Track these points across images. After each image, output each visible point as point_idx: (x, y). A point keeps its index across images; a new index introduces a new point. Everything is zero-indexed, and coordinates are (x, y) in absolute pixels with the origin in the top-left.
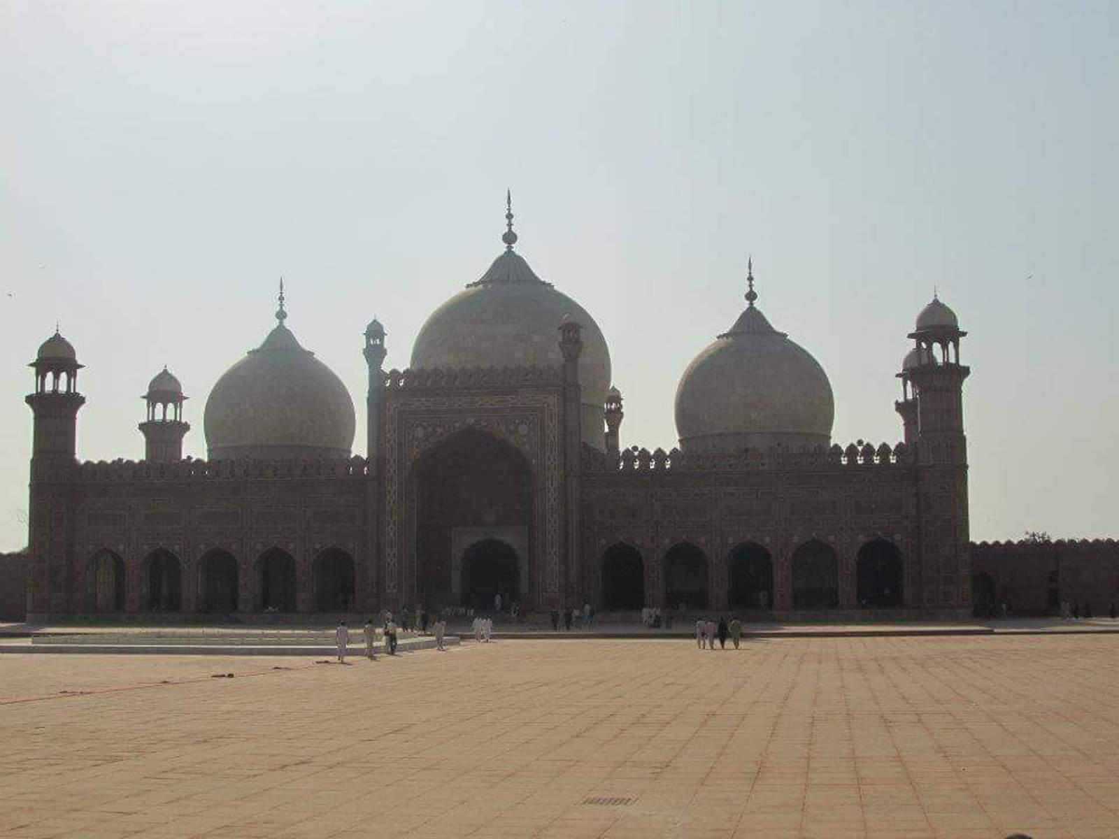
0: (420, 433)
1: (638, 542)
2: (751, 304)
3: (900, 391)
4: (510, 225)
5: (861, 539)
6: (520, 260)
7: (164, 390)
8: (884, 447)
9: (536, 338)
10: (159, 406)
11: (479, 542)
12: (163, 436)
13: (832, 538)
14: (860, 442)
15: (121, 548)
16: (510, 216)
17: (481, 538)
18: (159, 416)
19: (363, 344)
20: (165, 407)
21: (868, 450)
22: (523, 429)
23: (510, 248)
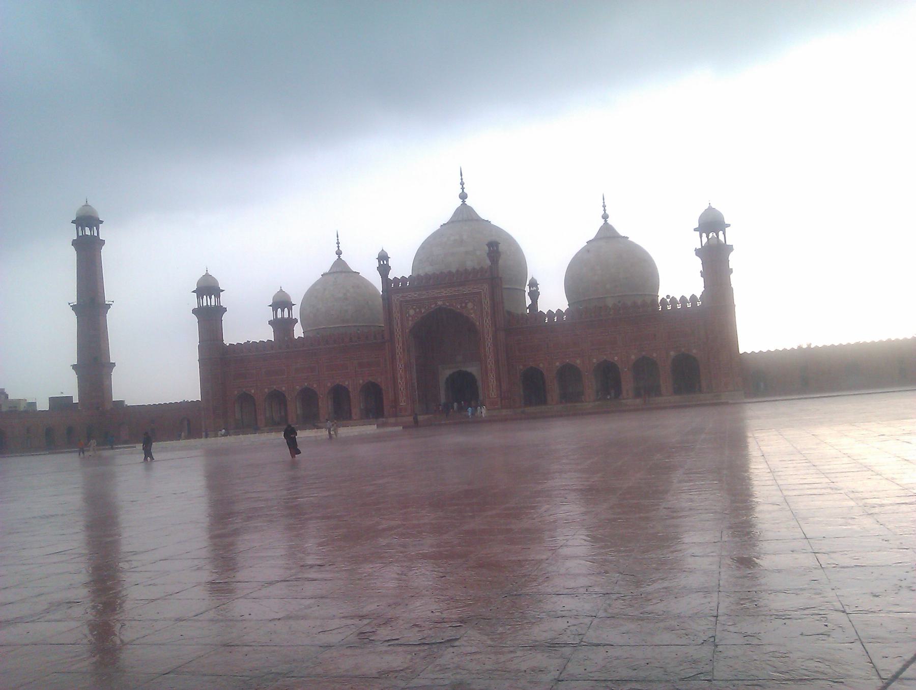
0: (412, 312)
1: (541, 365)
3: (697, 264)
4: (463, 189)
5: (672, 353)
6: (470, 210)
7: (281, 302)
8: (693, 297)
9: (478, 253)
11: (454, 373)
12: (282, 326)
13: (655, 355)
14: (668, 296)
16: (462, 184)
17: (455, 370)
18: (279, 316)
20: (283, 311)
21: (673, 300)
23: (464, 202)
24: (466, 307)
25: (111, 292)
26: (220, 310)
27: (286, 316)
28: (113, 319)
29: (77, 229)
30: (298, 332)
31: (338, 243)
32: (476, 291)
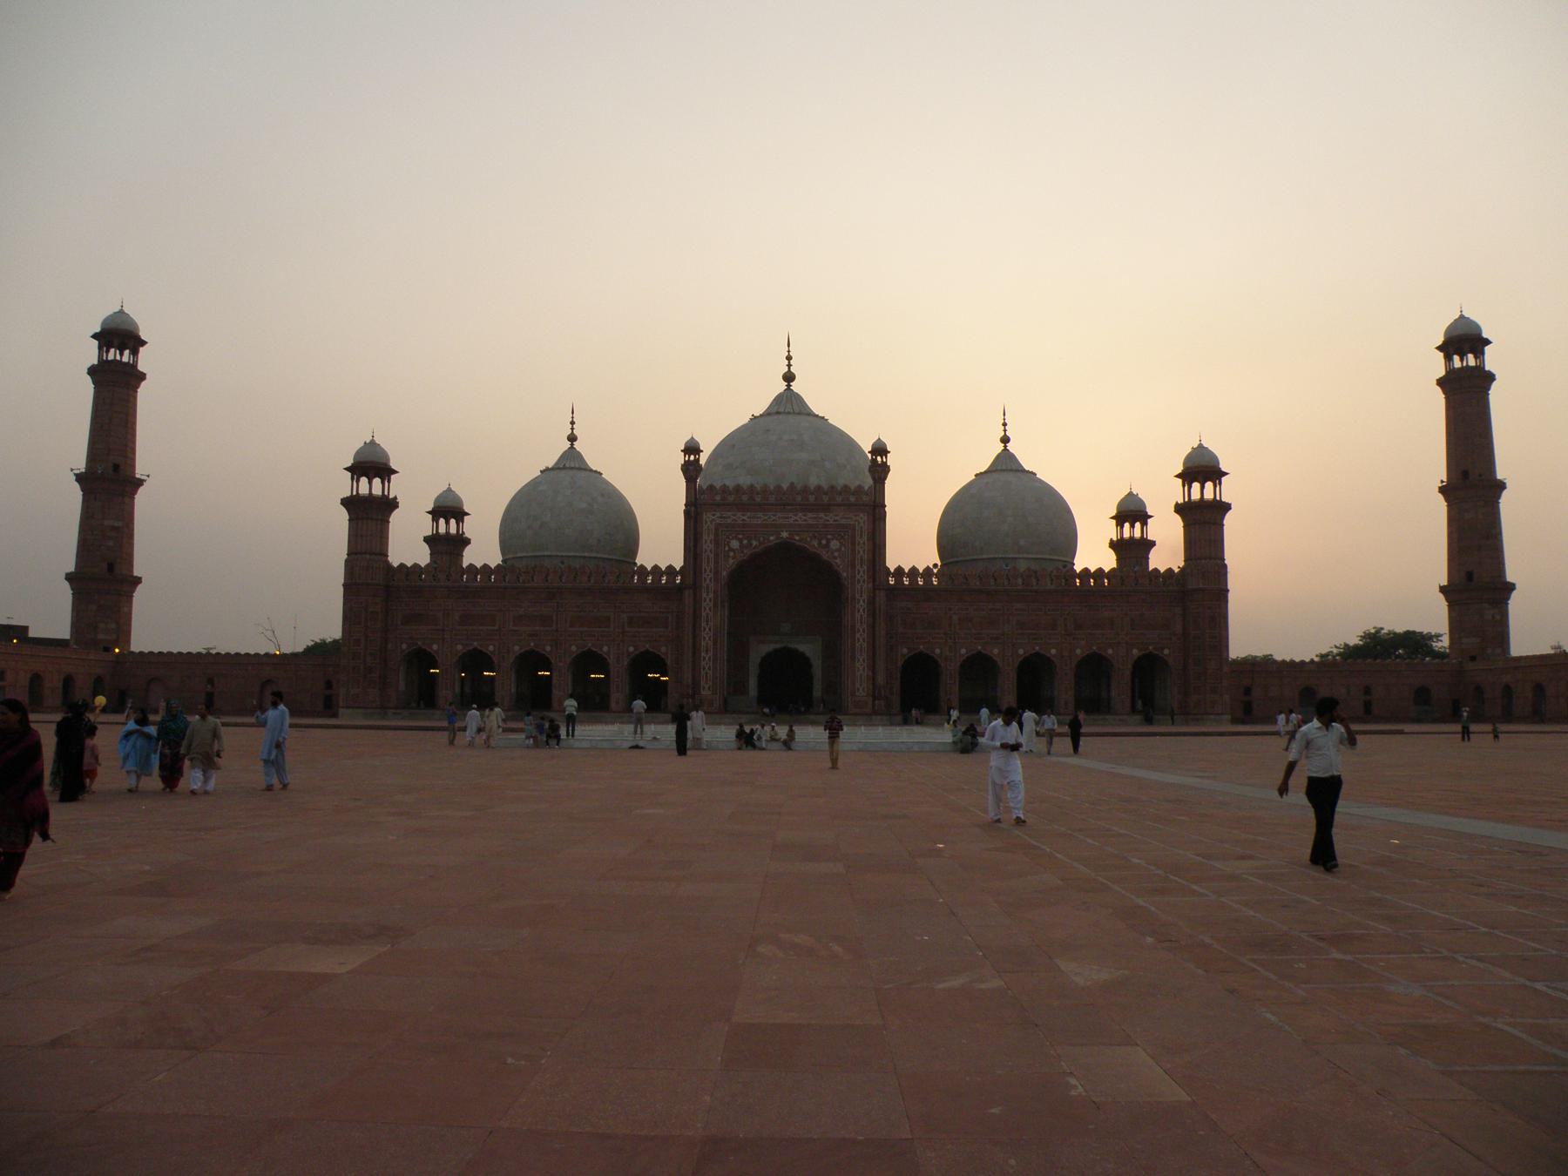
0: (735, 544)
1: (938, 651)
2: (1005, 448)
4: (789, 366)
6: (798, 397)
10: (442, 521)
11: (776, 651)
15: (435, 647)
16: (789, 358)
17: (778, 646)
18: (442, 530)
19: (680, 459)
20: (447, 523)
22: (835, 544)
24: (827, 545)
25: (147, 458)
26: (389, 504)
27: (453, 530)
28: (143, 501)
29: (100, 348)
30: (471, 557)
31: (573, 423)
32: (843, 522)
